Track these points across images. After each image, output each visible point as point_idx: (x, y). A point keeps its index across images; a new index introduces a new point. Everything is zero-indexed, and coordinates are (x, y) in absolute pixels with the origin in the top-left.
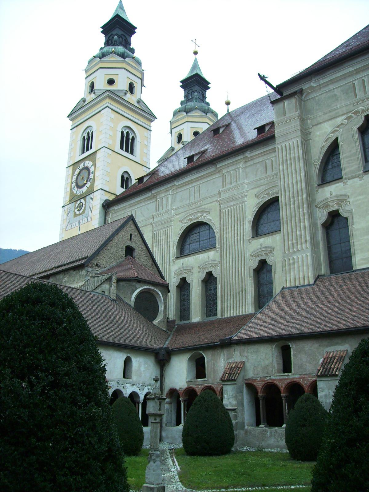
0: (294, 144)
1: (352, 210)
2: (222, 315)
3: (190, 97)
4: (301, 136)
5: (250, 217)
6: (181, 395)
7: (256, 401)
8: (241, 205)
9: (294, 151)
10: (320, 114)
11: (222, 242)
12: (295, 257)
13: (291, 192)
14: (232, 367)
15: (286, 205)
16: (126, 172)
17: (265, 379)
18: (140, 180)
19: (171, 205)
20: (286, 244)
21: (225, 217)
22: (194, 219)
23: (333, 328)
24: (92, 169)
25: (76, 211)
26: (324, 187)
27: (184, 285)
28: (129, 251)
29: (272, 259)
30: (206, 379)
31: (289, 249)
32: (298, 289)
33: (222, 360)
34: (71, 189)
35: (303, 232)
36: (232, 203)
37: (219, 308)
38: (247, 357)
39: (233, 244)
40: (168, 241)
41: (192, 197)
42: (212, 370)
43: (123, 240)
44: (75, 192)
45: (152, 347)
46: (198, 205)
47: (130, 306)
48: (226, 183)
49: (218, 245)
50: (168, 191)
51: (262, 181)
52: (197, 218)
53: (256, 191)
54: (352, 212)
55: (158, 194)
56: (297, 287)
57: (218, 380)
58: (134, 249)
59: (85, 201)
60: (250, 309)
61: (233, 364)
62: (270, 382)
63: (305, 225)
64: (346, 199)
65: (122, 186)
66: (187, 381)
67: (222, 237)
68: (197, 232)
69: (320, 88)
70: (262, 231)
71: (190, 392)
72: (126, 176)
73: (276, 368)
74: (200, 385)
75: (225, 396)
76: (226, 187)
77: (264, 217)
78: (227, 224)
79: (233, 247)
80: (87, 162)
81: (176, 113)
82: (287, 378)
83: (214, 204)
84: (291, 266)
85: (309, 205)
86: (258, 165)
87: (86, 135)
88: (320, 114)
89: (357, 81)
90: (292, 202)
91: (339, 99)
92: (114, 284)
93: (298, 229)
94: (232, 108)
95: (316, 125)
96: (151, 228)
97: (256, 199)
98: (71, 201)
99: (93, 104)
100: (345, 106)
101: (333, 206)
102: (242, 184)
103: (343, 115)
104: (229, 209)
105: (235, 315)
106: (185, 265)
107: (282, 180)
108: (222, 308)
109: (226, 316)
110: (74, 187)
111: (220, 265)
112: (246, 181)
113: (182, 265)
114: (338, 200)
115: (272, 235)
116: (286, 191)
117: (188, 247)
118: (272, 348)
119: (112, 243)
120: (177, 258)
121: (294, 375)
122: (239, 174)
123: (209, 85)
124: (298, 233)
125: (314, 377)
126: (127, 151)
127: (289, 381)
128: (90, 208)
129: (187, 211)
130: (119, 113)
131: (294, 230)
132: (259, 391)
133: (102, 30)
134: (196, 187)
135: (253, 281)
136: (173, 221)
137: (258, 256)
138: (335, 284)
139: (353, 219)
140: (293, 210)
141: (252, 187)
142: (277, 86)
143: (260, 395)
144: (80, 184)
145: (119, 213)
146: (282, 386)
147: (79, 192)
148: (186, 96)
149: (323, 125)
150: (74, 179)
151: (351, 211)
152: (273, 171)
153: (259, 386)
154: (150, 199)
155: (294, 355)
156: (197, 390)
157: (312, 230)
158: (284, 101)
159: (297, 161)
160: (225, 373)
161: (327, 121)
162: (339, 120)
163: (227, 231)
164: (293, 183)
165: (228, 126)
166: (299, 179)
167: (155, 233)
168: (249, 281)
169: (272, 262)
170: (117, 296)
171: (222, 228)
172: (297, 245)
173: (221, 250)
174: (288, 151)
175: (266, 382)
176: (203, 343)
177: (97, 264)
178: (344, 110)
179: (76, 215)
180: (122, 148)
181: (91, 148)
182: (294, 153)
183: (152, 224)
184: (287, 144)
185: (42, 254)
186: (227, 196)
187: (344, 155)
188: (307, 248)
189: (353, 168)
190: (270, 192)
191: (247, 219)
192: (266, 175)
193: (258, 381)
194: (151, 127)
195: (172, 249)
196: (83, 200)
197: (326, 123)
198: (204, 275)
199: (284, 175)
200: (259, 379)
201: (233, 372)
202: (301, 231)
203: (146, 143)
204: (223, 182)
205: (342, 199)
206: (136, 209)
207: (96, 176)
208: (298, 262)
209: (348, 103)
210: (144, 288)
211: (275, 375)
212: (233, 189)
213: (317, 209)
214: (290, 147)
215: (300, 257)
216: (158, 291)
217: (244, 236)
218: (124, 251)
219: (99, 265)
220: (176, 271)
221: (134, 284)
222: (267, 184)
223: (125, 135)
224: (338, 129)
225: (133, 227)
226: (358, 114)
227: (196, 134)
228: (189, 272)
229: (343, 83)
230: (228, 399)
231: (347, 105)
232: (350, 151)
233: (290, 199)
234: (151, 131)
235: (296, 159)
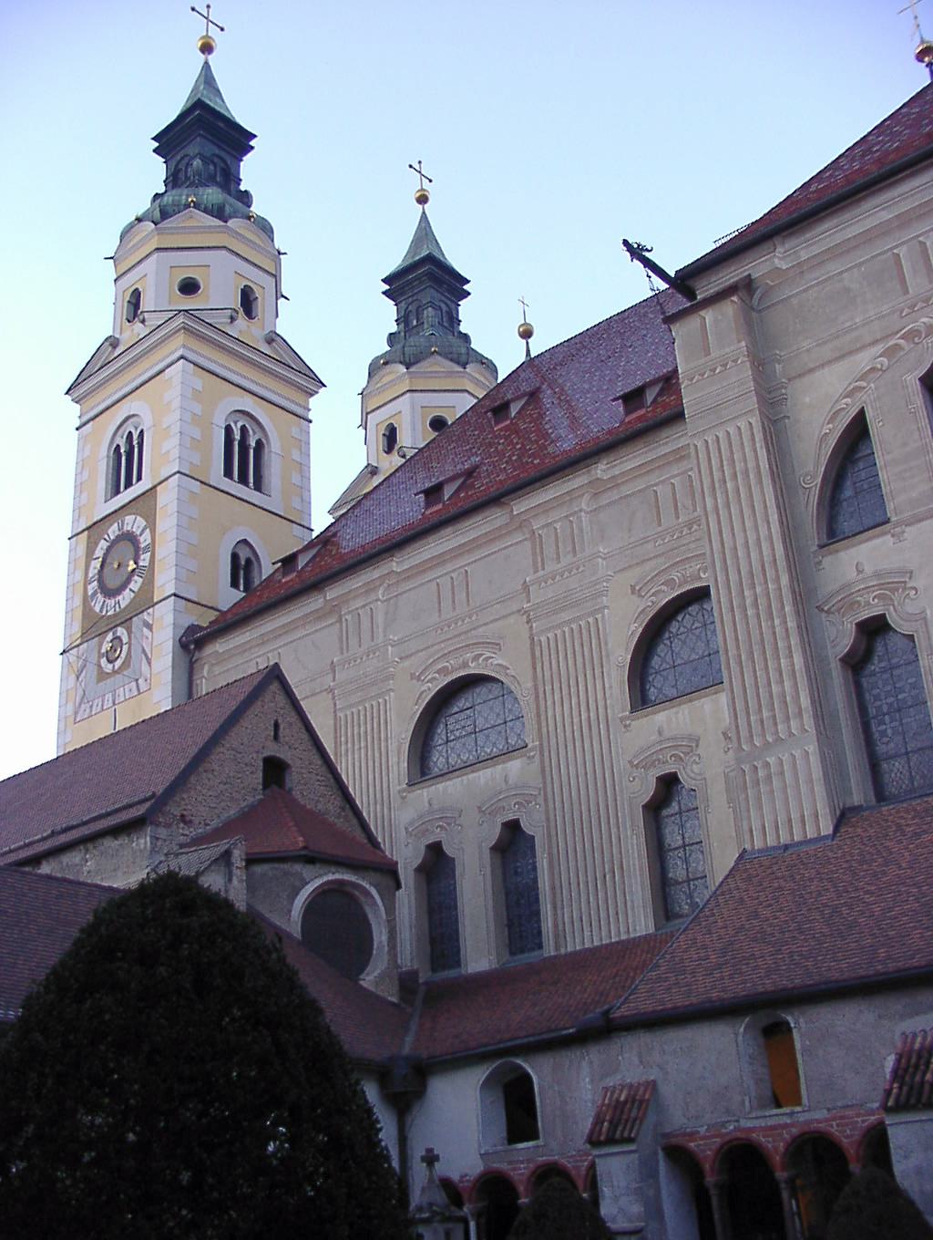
0: (740, 434)
3: (415, 323)
4: (759, 410)
5: (621, 652)
7: (700, 1198)
8: (591, 620)
9: (744, 454)
12: (771, 760)
14: (617, 1100)
15: (732, 610)
16: (245, 541)
17: (724, 1131)
18: (289, 562)
19: (385, 632)
21: (546, 658)
23: (915, 962)
24: (145, 540)
25: (104, 661)
26: (837, 551)
28: (275, 770)
29: (696, 771)
30: (540, 1142)
32: (789, 852)
33: (587, 1080)
34: (86, 600)
35: (787, 684)
36: (565, 616)
37: (547, 925)
38: (661, 1067)
41: (446, 604)
42: (558, 1113)
43: (252, 740)
44: (97, 609)
46: (464, 628)
48: (542, 560)
50: (375, 589)
51: (650, 546)
52: (465, 665)
53: (632, 576)
54: (925, 619)
55: (344, 599)
56: (786, 847)
57: (580, 1142)
59: (129, 633)
61: (622, 1091)
62: (737, 1139)
63: (793, 664)
64: (905, 582)
65: (235, 584)
66: (482, 1152)
67: (543, 717)
68: (468, 705)
70: (660, 690)
71: (494, 1187)
73: (753, 1094)
75: (606, 1191)
76: (543, 569)
77: (661, 649)
79: (578, 744)
80: (129, 519)
81: (375, 368)
82: (788, 1121)
83: (512, 620)
84: (763, 788)
85: (800, 606)
87: (122, 442)
88: (805, 344)
89: (905, 248)
90: (748, 602)
92: (238, 872)
94: (539, 345)
96: (331, 703)
97: (634, 598)
98: (86, 635)
99: (139, 349)
100: (878, 319)
103: (875, 342)
104: (559, 632)
105: (596, 943)
107: (715, 537)
108: (556, 926)
109: (569, 949)
110: (95, 594)
111: (541, 800)
113: (427, 805)
115: (690, 701)
118: (736, 1035)
119: (222, 753)
121: (811, 1112)
122: (581, 530)
123: (466, 287)
125: (874, 1115)
126: (243, 480)
127: (794, 1130)
128: (144, 651)
129: (432, 646)
132: (707, 1166)
135: (643, 840)
136: (392, 677)
137: (653, 764)
138: (895, 832)
143: (710, 1180)
144: (112, 583)
146: (776, 1147)
147: (110, 607)
148: (402, 320)
150: (93, 572)
151: (923, 615)
152: (678, 518)
153: (706, 1150)
154: (319, 618)
155: (804, 1050)
156: (516, 1178)
157: (813, 676)
158: (702, 313)
159: (753, 482)
160: (598, 1121)
162: (864, 360)
163: (557, 697)
165: (533, 395)
166: (763, 531)
168: (632, 839)
169: (694, 779)
173: (542, 755)
175: (727, 1138)
177: (182, 816)
179: (102, 676)
180: (228, 473)
181: (139, 478)
182: (745, 461)
183: (331, 690)
184: (721, 435)
187: (888, 457)
190: (676, 575)
192: (660, 529)
193: (702, 1138)
194: (309, 410)
195: (396, 759)
196: (121, 631)
197: (826, 369)
198: (496, 832)
199: (719, 523)
200: (703, 1130)
201: (625, 1117)
203: (296, 455)
204: (534, 554)
205: (896, 582)
206: (280, 647)
207: (157, 557)
208: (782, 773)
209: (885, 309)
210: (325, 879)
211: (754, 1115)
212: (566, 574)
213: (824, 615)
214: (730, 444)
216: (368, 886)
219: (188, 819)
220: (411, 824)
221: (298, 867)
222: (663, 553)
224: (864, 384)
225: (281, 700)
226: (916, 340)
227: (438, 424)
228: (449, 824)
229: (863, 255)
230: (616, 1199)
232: (905, 444)
234: (311, 422)
235: (752, 476)
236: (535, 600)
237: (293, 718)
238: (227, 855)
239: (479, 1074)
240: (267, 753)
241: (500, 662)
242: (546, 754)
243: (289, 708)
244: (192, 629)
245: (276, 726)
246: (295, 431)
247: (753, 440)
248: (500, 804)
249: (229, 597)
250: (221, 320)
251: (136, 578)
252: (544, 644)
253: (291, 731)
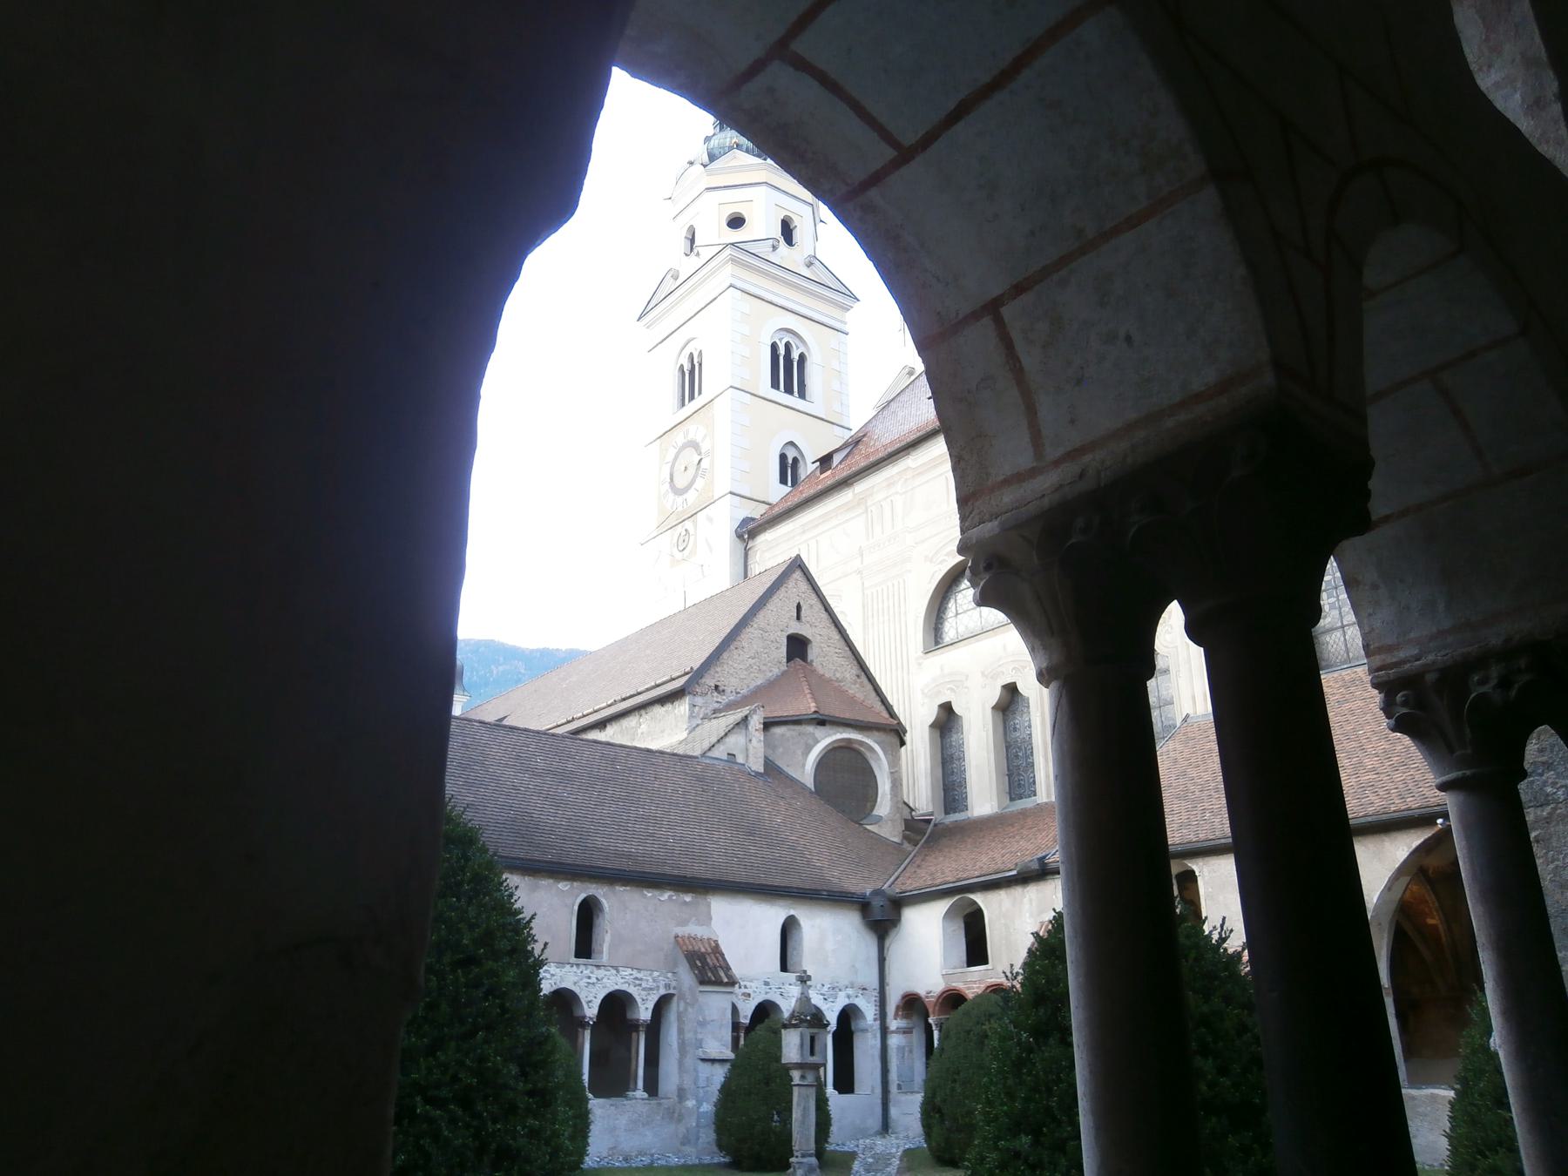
16: (791, 443)
18: (825, 461)
24: (704, 447)
28: (797, 646)
43: (778, 622)
45: (853, 889)
47: (803, 787)
65: (783, 481)
119: (751, 632)
126: (789, 390)
144: (680, 482)
145: (773, 550)
170: (769, 765)
177: (717, 687)
180: (775, 385)
196: (688, 524)
218: (784, 649)
223: (782, 351)
225: (804, 586)
237: (814, 600)
238: (745, 719)
239: (942, 906)
240: (791, 631)
243: (810, 591)
245: (799, 607)
249: (777, 492)
250: (763, 249)
253: (812, 610)
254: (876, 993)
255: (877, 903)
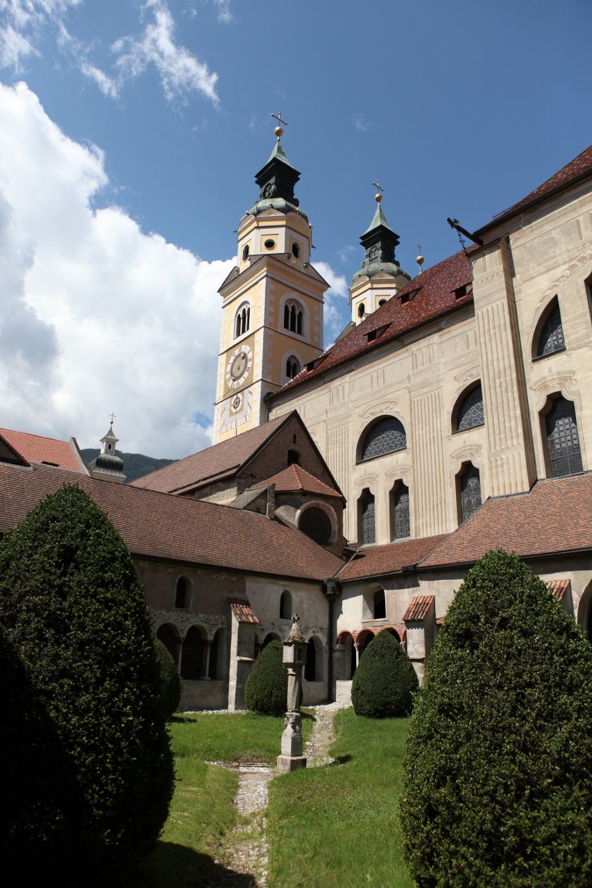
1: (579, 390)
2: (416, 536)
6: (355, 640)
10: (532, 265)
11: (414, 440)
12: (504, 457)
13: (496, 371)
20: (492, 439)
22: (377, 413)
24: (250, 356)
25: (232, 408)
27: (366, 499)
31: (495, 446)
36: (425, 390)
37: (412, 526)
38: (438, 590)
39: (428, 443)
40: (346, 441)
41: (375, 384)
46: (382, 395)
49: (408, 445)
51: (463, 359)
52: (382, 411)
54: (579, 394)
56: (508, 496)
58: (299, 454)
59: (243, 396)
60: (451, 526)
69: (532, 230)
71: (366, 636)
72: (293, 362)
74: (378, 626)
78: (420, 417)
80: (243, 347)
83: (402, 391)
84: (499, 469)
86: (457, 339)
87: (240, 313)
89: (581, 217)
90: (497, 385)
91: (558, 243)
93: (507, 419)
95: (528, 280)
96: (325, 426)
97: (456, 382)
99: (249, 273)
101: (553, 387)
102: (438, 364)
103: (564, 263)
104: (422, 397)
105: (433, 535)
106: (367, 472)
107: (484, 356)
108: (416, 527)
109: (421, 537)
112: (442, 360)
114: (560, 378)
116: (490, 370)
117: (372, 447)
120: (357, 464)
123: (398, 240)
124: (507, 425)
126: (293, 329)
130: (281, 283)
131: (502, 421)
133: (256, 179)
134: (378, 372)
137: (461, 457)
139: (581, 403)
140: (499, 394)
141: (451, 367)
142: (475, 234)
144: (237, 374)
149: (537, 279)
160: (408, 612)
161: (542, 274)
162: (559, 272)
163: (420, 425)
164: (498, 359)
166: (506, 353)
167: (329, 432)
171: (414, 422)
172: (506, 441)
174: (491, 318)
176: (382, 572)
177: (252, 475)
178: (566, 257)
179: (232, 414)
180: (286, 326)
181: (248, 329)
182: (499, 320)
183: (325, 421)
184: (490, 309)
185: (188, 463)
186: (419, 380)
187: (567, 318)
188: (519, 444)
189: (579, 335)
190: (474, 372)
191: (445, 409)
196: (239, 395)
198: (392, 484)
199: (486, 348)
202: (510, 421)
203: (317, 319)
204: (413, 363)
208: (508, 463)
209: (571, 247)
214: (493, 313)
215: (510, 456)
217: (441, 431)
218: (287, 457)
222: (469, 362)
224: (558, 283)
225: (297, 426)
231: (570, 251)
232: (575, 312)
233: (495, 381)
234: (324, 303)
236: (413, 382)
237: (302, 433)
240: (290, 449)
241: (397, 410)
242: (415, 450)
244: (269, 394)
245: (295, 436)
246: (316, 308)
247: (504, 311)
248: (394, 473)
250: (284, 259)
251: (246, 372)
252: (416, 402)
254: (327, 631)
255: (330, 585)
